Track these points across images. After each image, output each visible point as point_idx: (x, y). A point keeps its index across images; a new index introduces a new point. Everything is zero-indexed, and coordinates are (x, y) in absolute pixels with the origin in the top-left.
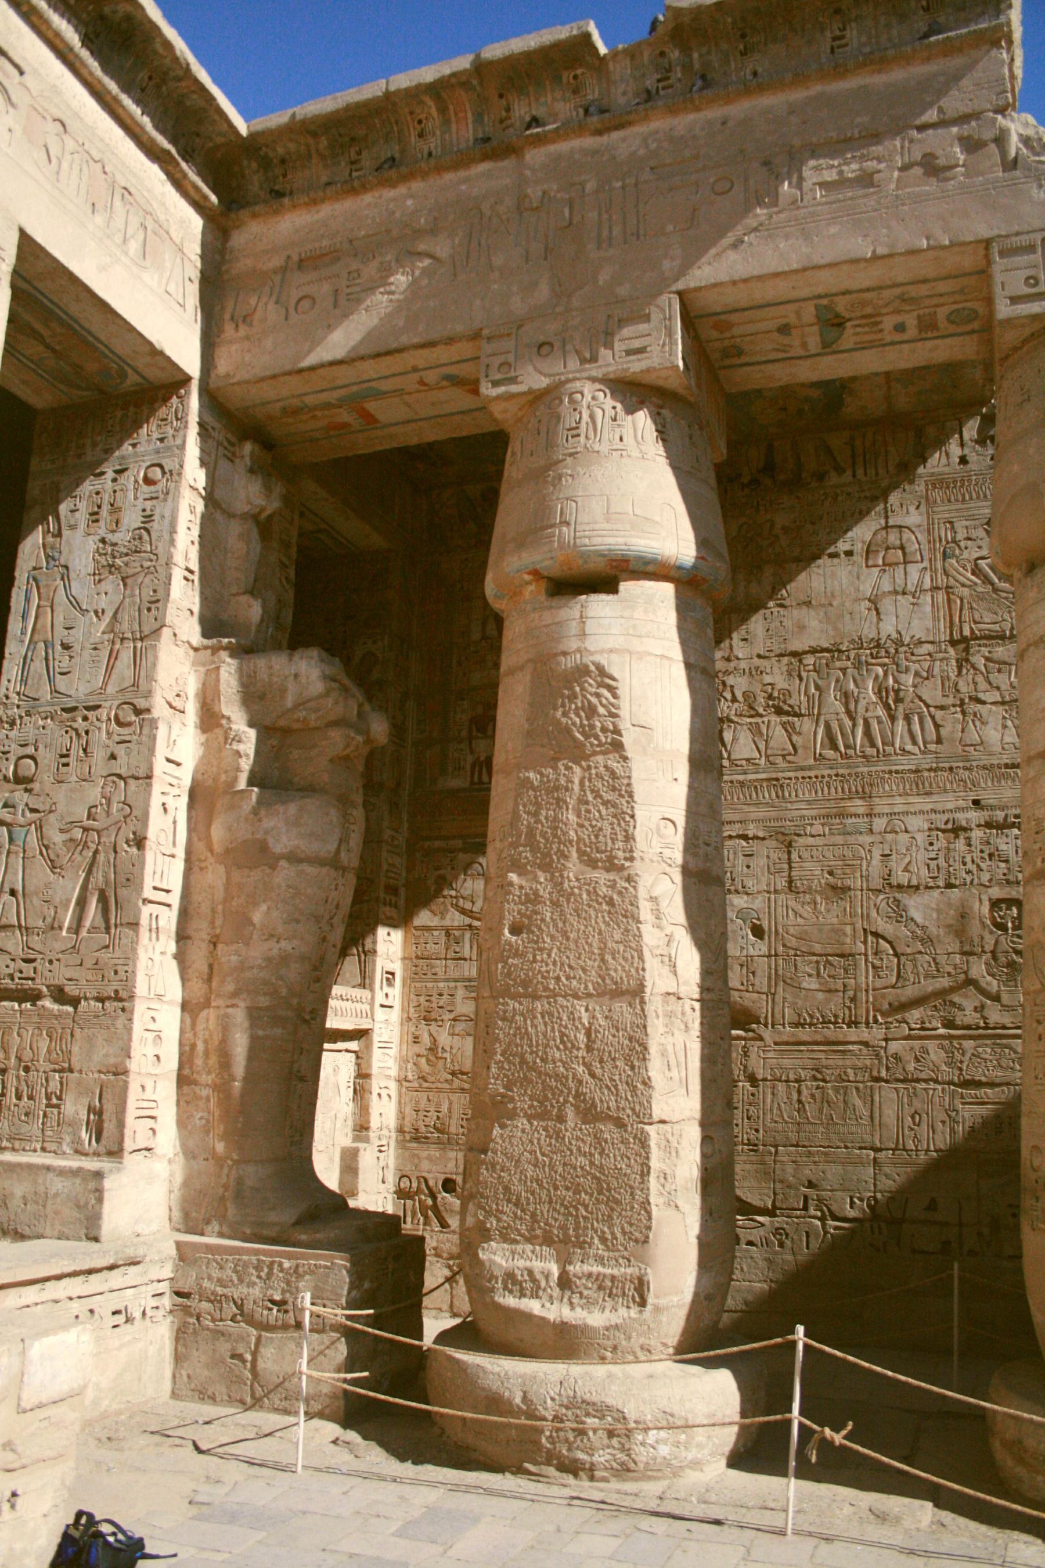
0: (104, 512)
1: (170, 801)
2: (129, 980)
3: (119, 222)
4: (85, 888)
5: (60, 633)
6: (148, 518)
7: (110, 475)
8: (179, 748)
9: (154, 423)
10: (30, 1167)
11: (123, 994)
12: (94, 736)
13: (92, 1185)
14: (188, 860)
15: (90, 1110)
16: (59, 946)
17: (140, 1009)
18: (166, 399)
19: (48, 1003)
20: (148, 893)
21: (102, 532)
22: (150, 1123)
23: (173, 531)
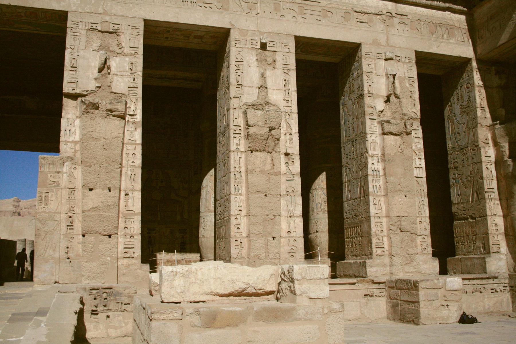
0: (460, 98)
1: (488, 166)
2: (485, 212)
3: (440, 32)
4: (473, 191)
5: (457, 130)
6: (469, 97)
7: (459, 88)
8: (489, 153)
9: (466, 72)
10: (470, 258)
11: (485, 215)
12: (468, 154)
13: (483, 260)
14: (497, 180)
15: (482, 243)
16: (470, 206)
17: (489, 218)
18: (467, 66)
19: (470, 220)
20: (486, 190)
21: (460, 103)
22: (498, 246)
23: (475, 99)
